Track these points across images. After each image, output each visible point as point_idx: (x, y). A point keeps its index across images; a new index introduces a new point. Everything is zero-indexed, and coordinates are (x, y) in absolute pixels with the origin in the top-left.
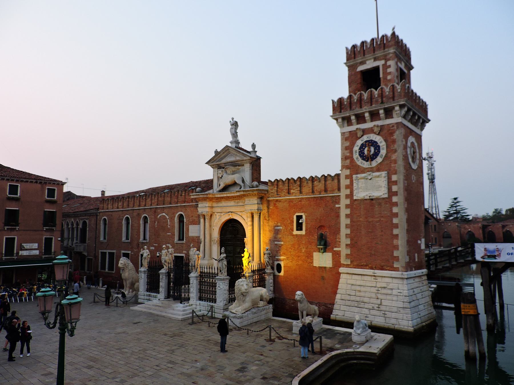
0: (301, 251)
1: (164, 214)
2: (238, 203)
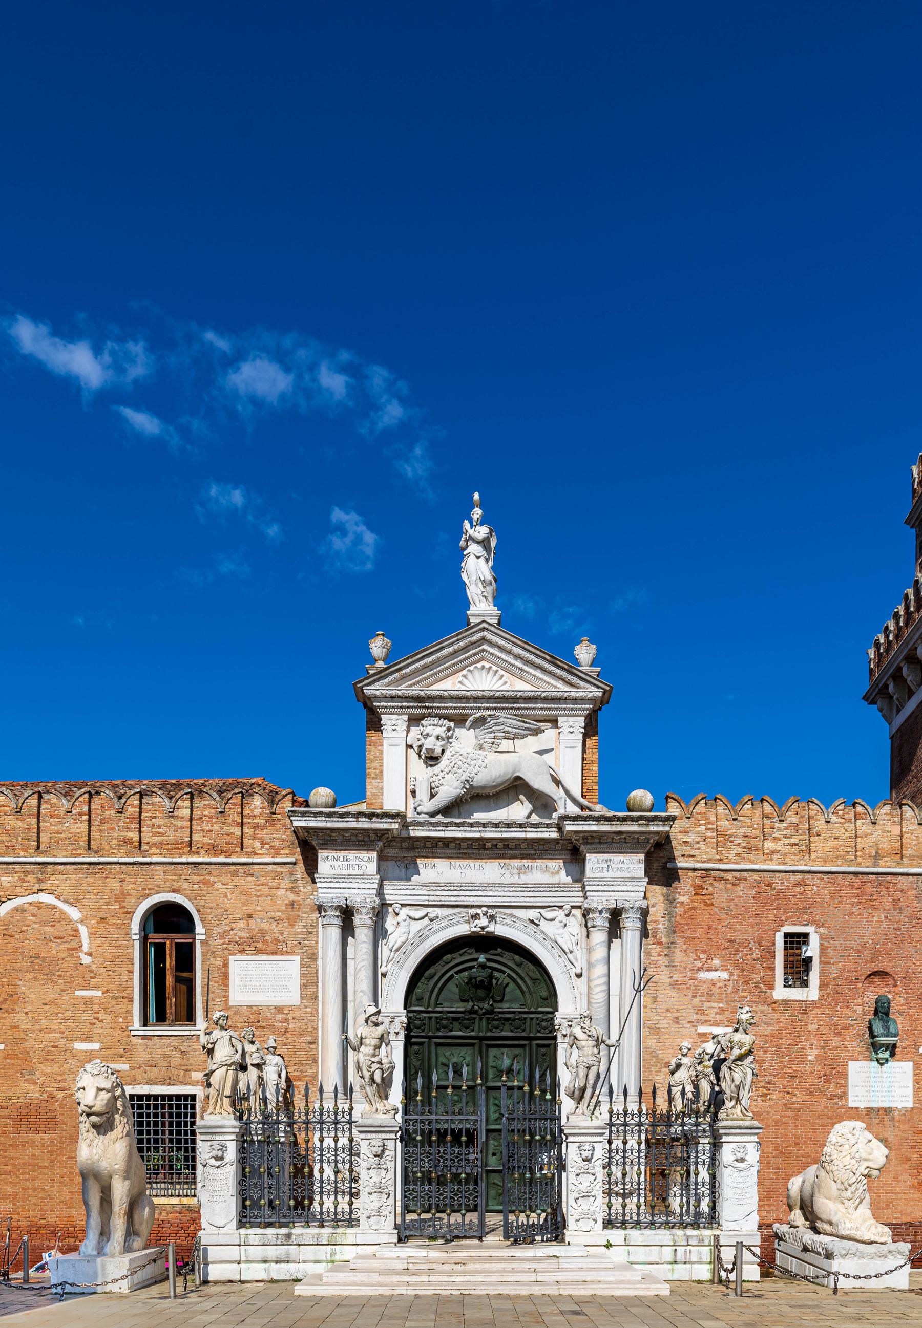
0: (801, 1058)
1: (44, 898)
2: (520, 871)
